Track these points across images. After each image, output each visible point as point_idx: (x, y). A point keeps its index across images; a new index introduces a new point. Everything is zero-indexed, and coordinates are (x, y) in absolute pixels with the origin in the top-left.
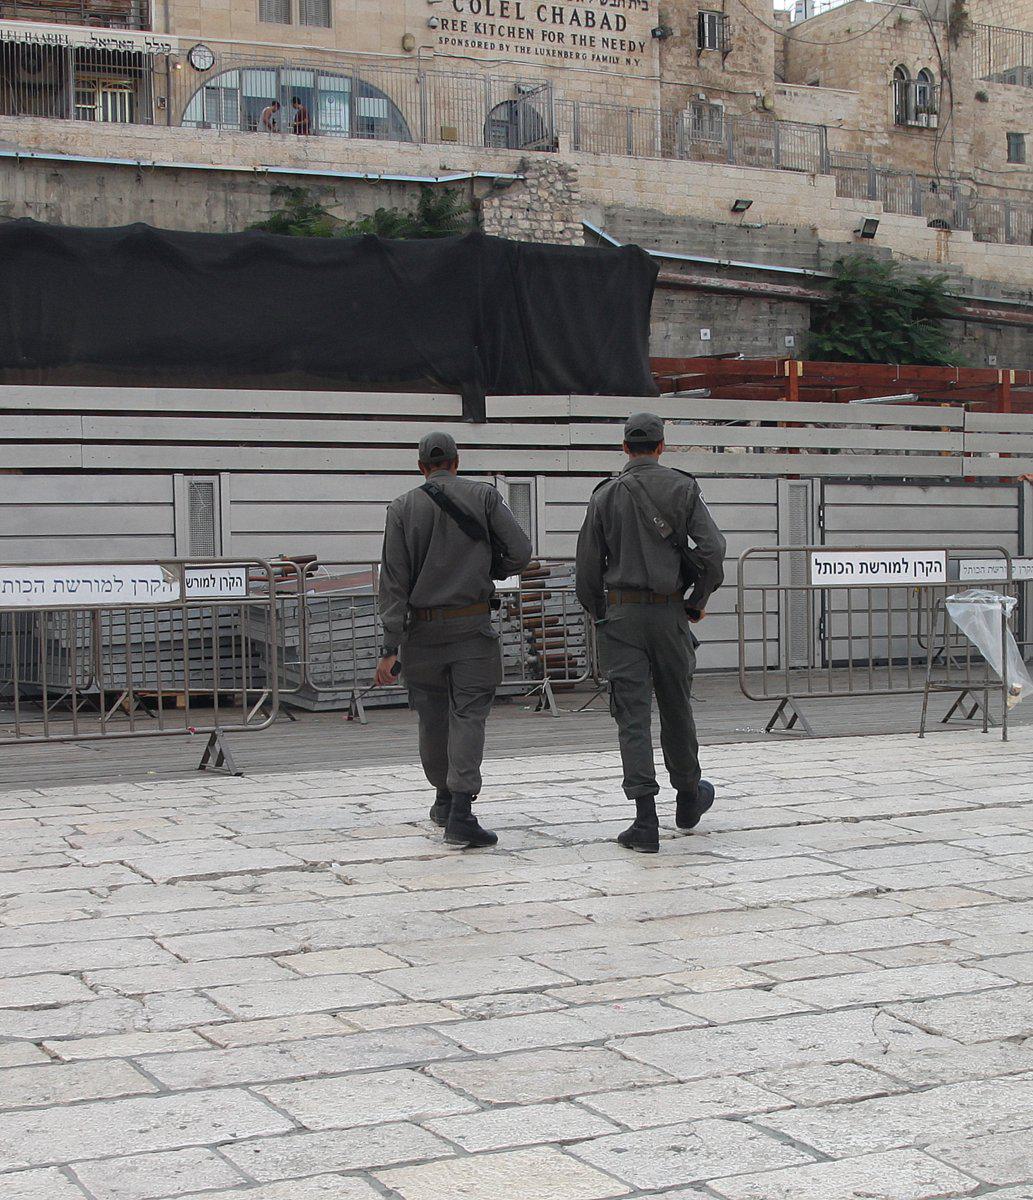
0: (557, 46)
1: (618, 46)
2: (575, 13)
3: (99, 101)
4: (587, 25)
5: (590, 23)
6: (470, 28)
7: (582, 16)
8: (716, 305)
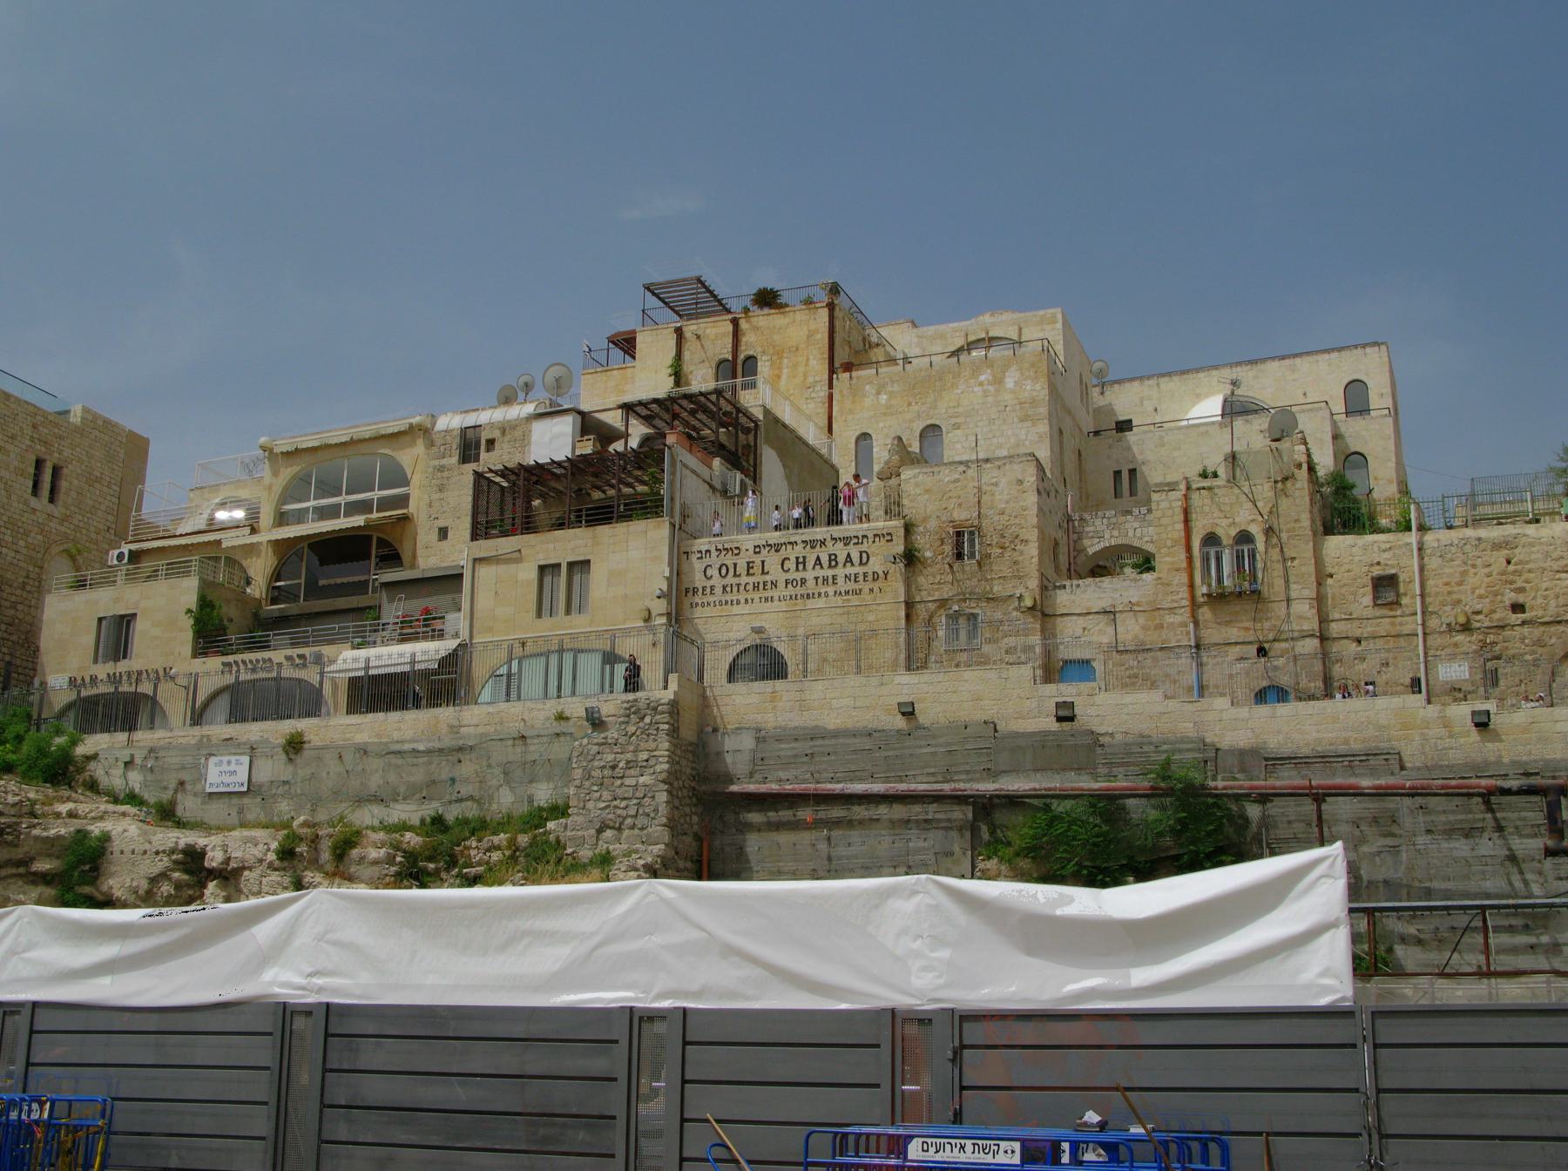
0: (800, 590)
1: (861, 578)
2: (818, 558)
4: (830, 566)
5: (833, 563)
6: (718, 590)
7: (825, 560)
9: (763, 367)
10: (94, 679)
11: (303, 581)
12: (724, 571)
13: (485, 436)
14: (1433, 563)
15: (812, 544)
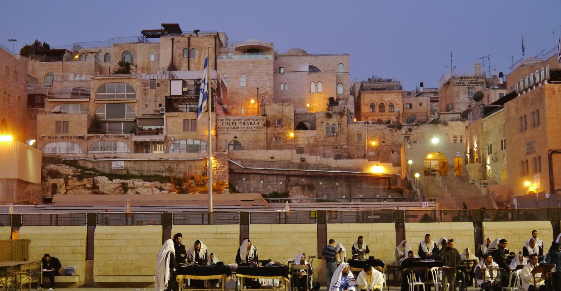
0: (244, 129)
3: (158, 147)
6: (226, 128)
8: (265, 177)
9: (197, 52)
10: (56, 138)
11: (105, 113)
12: (227, 124)
13: (157, 82)
14: (369, 132)
15: (247, 120)
